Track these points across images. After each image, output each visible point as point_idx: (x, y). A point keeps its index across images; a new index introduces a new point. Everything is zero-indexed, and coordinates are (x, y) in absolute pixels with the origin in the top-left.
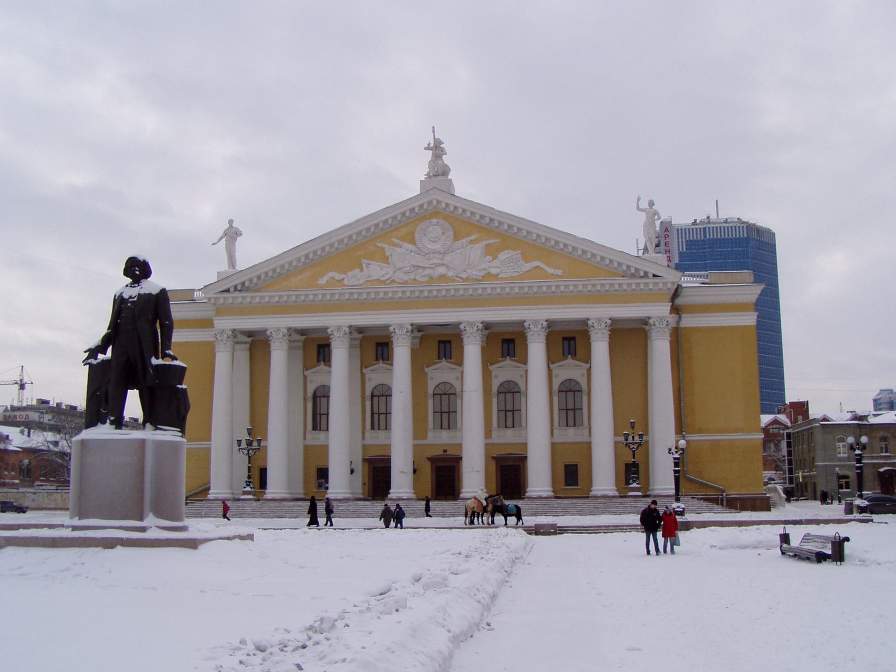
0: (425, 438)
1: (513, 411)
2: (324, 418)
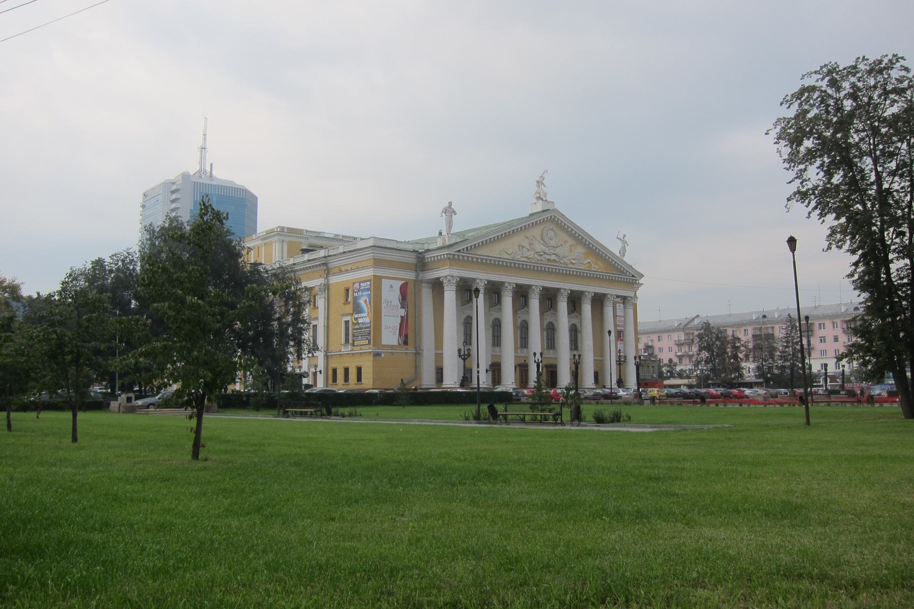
0: (517, 353)
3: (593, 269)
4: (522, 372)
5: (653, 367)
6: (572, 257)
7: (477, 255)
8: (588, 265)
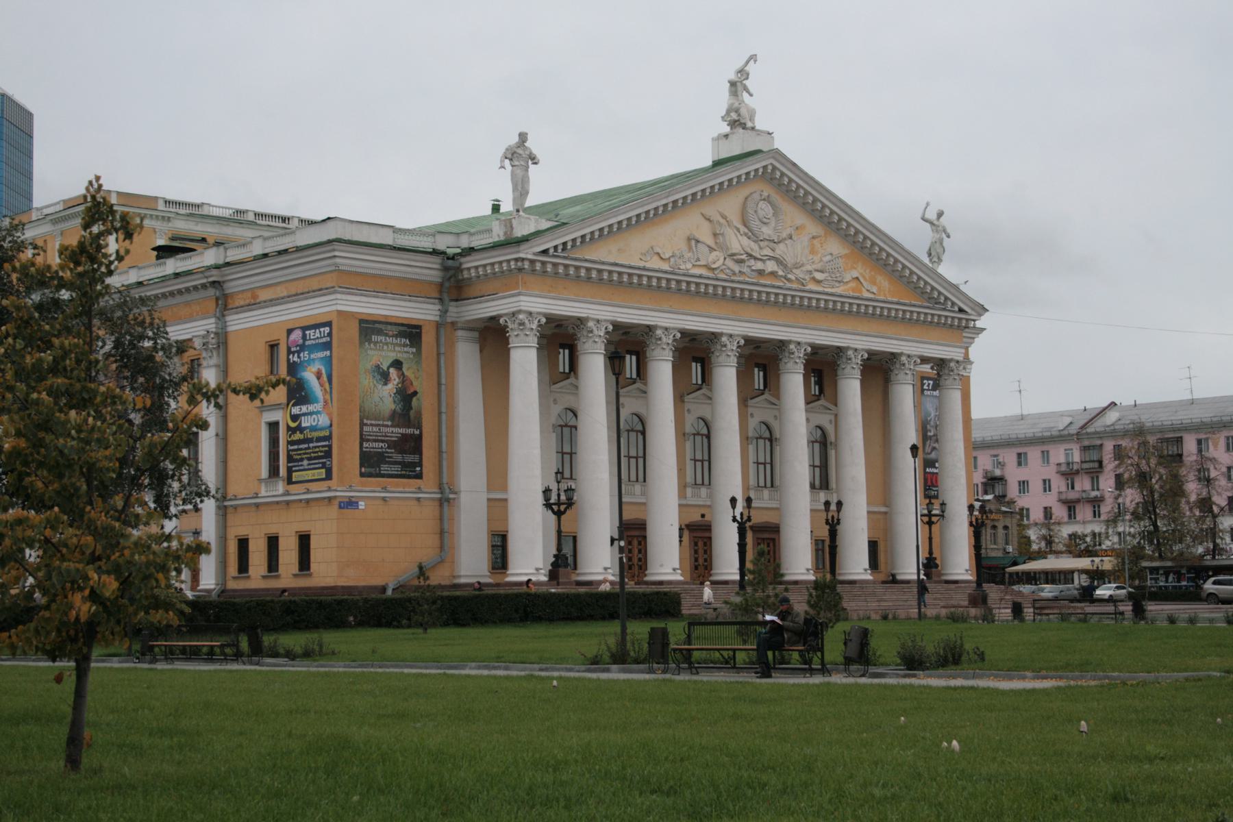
4: (696, 544)
5: (1006, 528)
6: (814, 266)
7: (586, 260)
8: (853, 285)
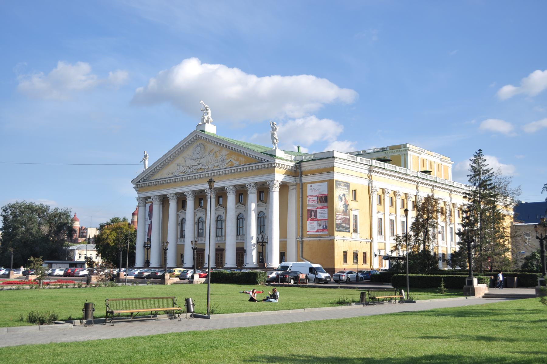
1: (263, 226)
2: (184, 232)
3: (235, 165)
